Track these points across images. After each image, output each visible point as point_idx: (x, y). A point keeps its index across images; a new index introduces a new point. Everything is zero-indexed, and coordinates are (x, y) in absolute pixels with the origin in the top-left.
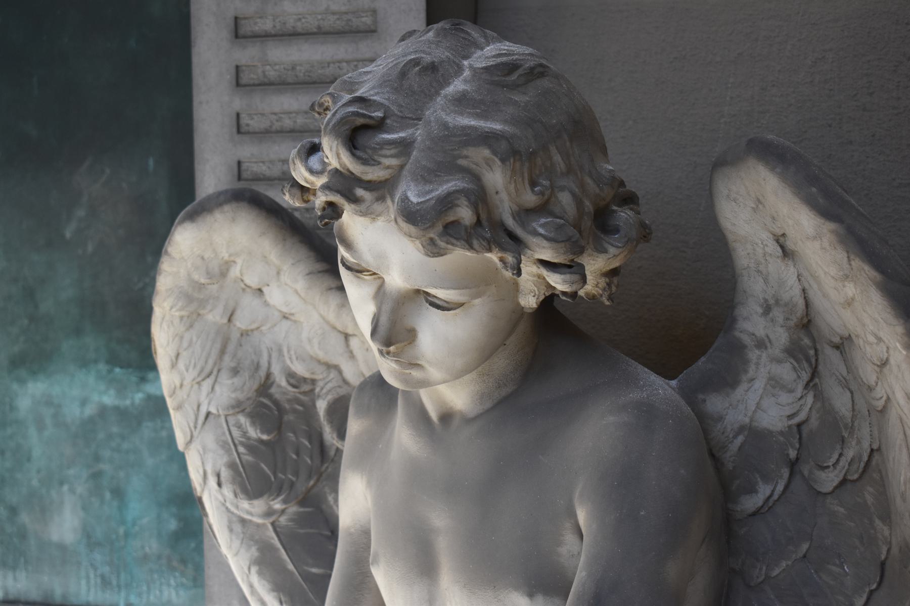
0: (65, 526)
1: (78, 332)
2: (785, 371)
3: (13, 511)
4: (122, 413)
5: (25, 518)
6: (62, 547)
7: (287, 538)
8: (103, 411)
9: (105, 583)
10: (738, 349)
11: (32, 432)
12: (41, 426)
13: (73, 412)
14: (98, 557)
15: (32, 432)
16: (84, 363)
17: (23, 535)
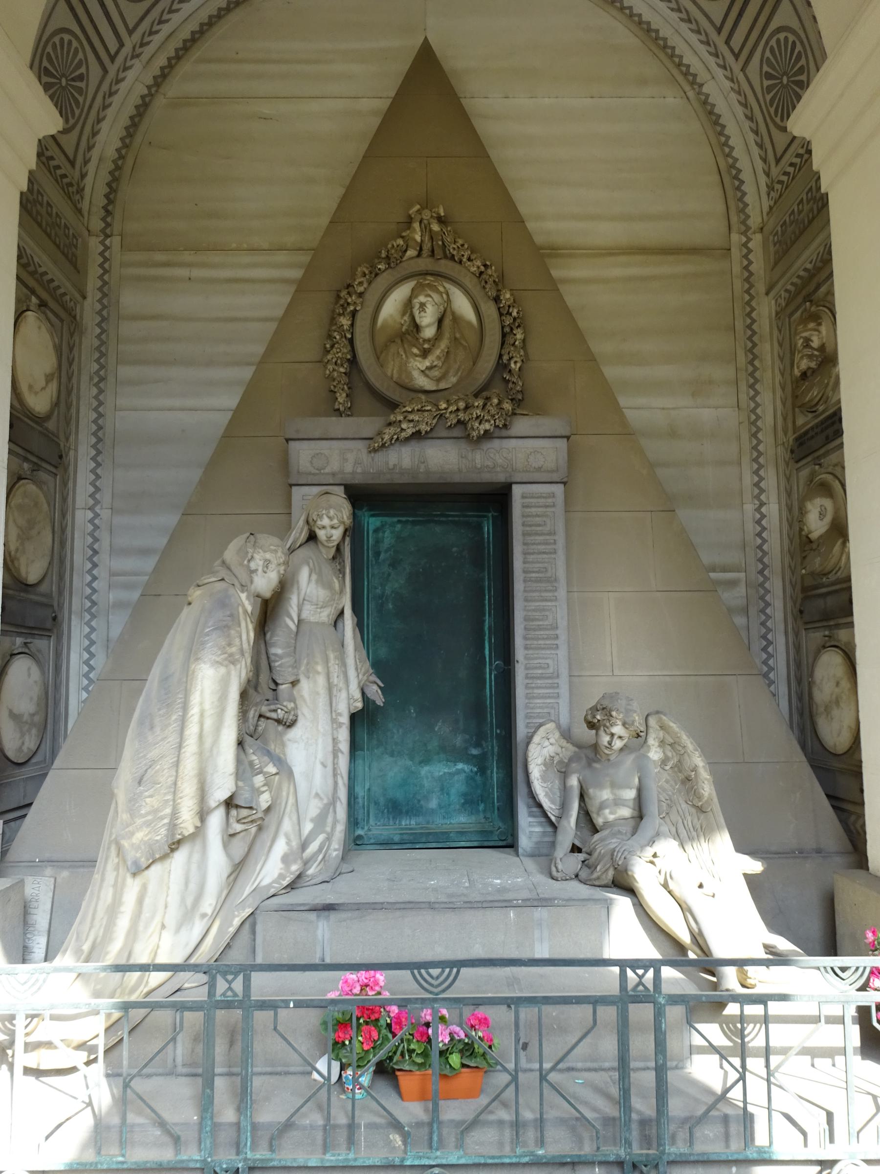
0: (433, 804)
1: (438, 753)
2: (658, 749)
3: (419, 801)
4: (450, 774)
5: (422, 802)
6: (432, 810)
7: (550, 790)
8: (445, 773)
9: (444, 818)
10: (649, 746)
11: (425, 780)
12: (427, 778)
13: (436, 774)
14: (442, 811)
15: (425, 780)
16: (440, 762)
17: (421, 807)
